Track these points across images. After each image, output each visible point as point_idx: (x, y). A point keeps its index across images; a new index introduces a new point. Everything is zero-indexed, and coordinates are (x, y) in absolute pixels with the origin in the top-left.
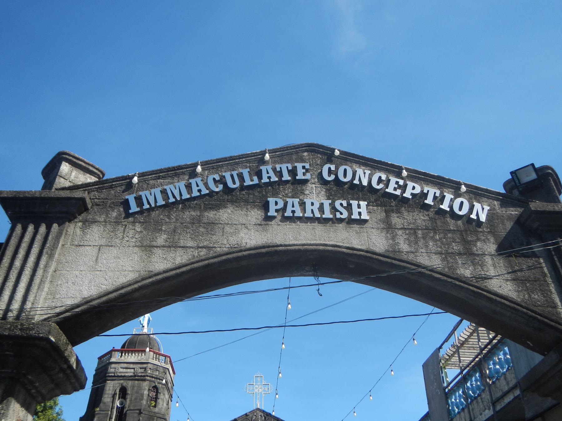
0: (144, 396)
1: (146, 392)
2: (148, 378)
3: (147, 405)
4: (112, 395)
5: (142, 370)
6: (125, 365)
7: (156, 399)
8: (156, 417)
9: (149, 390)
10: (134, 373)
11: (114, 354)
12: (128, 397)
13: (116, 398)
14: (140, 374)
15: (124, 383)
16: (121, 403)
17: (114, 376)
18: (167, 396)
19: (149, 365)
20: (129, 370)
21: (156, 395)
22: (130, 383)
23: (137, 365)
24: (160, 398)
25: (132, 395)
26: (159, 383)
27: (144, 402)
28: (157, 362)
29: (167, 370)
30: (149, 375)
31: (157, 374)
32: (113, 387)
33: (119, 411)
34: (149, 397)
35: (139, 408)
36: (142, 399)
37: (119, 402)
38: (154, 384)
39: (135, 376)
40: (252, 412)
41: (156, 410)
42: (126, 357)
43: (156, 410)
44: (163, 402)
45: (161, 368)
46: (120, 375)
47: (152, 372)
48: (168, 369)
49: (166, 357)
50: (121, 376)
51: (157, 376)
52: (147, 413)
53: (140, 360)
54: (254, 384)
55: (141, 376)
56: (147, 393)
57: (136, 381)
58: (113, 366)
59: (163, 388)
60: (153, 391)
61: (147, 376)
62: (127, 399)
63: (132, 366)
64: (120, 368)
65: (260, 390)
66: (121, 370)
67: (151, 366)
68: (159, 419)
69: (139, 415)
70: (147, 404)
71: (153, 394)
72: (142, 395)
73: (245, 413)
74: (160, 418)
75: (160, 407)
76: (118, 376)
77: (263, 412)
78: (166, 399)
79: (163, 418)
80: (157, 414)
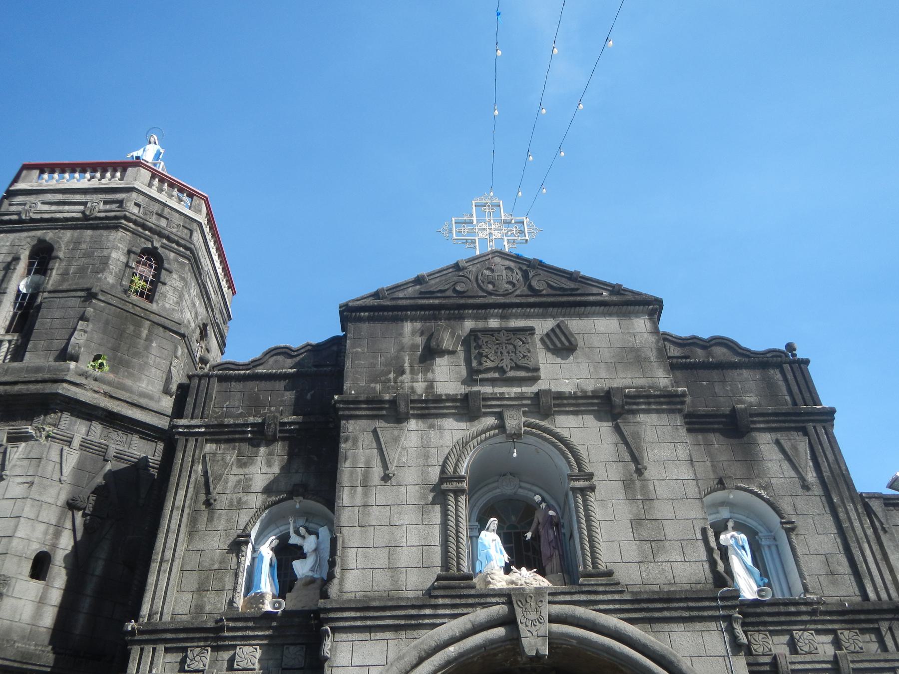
0: (110, 262)
1: (118, 256)
2: (131, 225)
3: (119, 287)
4: (4, 265)
5: (114, 206)
6: (59, 197)
7: (156, 282)
8: (149, 322)
9: (129, 252)
10: (83, 213)
11: (26, 176)
13: (15, 269)
14: (102, 215)
15: (49, 235)
16: (36, 290)
17: (20, 221)
18: (201, 310)
19: (134, 195)
20: (67, 208)
21: (157, 276)
22: (68, 234)
23: (95, 196)
24: (169, 283)
25: (70, 260)
26: (166, 248)
27: (111, 280)
28: (162, 197)
29: (195, 226)
30: (134, 217)
31: (163, 223)
32: (12, 246)
33: (21, 305)
34: (128, 270)
35: (86, 286)
36: (102, 271)
37: (27, 282)
38: (150, 243)
39: (86, 217)
40: (476, 261)
41: (154, 307)
42: (65, 180)
43: (154, 307)
44: (181, 297)
45: (177, 215)
46: (38, 216)
47: (145, 214)
48: (200, 225)
49: (195, 197)
50: (42, 220)
51: (162, 230)
52: (114, 302)
54: (475, 219)
55: (107, 218)
56: (123, 259)
57: (89, 231)
58: (20, 199)
59: (182, 265)
60: (144, 264)
61: (126, 218)
62: (52, 269)
63: (78, 198)
64: (39, 204)
65: (497, 235)
66: (40, 207)
68: (161, 328)
69: (83, 301)
70: (121, 285)
71: (148, 272)
72: (105, 262)
73: (452, 262)
74: (165, 328)
75: (167, 306)
76: (32, 220)
77: (518, 259)
78: (194, 305)
79: (174, 329)
80: (152, 315)
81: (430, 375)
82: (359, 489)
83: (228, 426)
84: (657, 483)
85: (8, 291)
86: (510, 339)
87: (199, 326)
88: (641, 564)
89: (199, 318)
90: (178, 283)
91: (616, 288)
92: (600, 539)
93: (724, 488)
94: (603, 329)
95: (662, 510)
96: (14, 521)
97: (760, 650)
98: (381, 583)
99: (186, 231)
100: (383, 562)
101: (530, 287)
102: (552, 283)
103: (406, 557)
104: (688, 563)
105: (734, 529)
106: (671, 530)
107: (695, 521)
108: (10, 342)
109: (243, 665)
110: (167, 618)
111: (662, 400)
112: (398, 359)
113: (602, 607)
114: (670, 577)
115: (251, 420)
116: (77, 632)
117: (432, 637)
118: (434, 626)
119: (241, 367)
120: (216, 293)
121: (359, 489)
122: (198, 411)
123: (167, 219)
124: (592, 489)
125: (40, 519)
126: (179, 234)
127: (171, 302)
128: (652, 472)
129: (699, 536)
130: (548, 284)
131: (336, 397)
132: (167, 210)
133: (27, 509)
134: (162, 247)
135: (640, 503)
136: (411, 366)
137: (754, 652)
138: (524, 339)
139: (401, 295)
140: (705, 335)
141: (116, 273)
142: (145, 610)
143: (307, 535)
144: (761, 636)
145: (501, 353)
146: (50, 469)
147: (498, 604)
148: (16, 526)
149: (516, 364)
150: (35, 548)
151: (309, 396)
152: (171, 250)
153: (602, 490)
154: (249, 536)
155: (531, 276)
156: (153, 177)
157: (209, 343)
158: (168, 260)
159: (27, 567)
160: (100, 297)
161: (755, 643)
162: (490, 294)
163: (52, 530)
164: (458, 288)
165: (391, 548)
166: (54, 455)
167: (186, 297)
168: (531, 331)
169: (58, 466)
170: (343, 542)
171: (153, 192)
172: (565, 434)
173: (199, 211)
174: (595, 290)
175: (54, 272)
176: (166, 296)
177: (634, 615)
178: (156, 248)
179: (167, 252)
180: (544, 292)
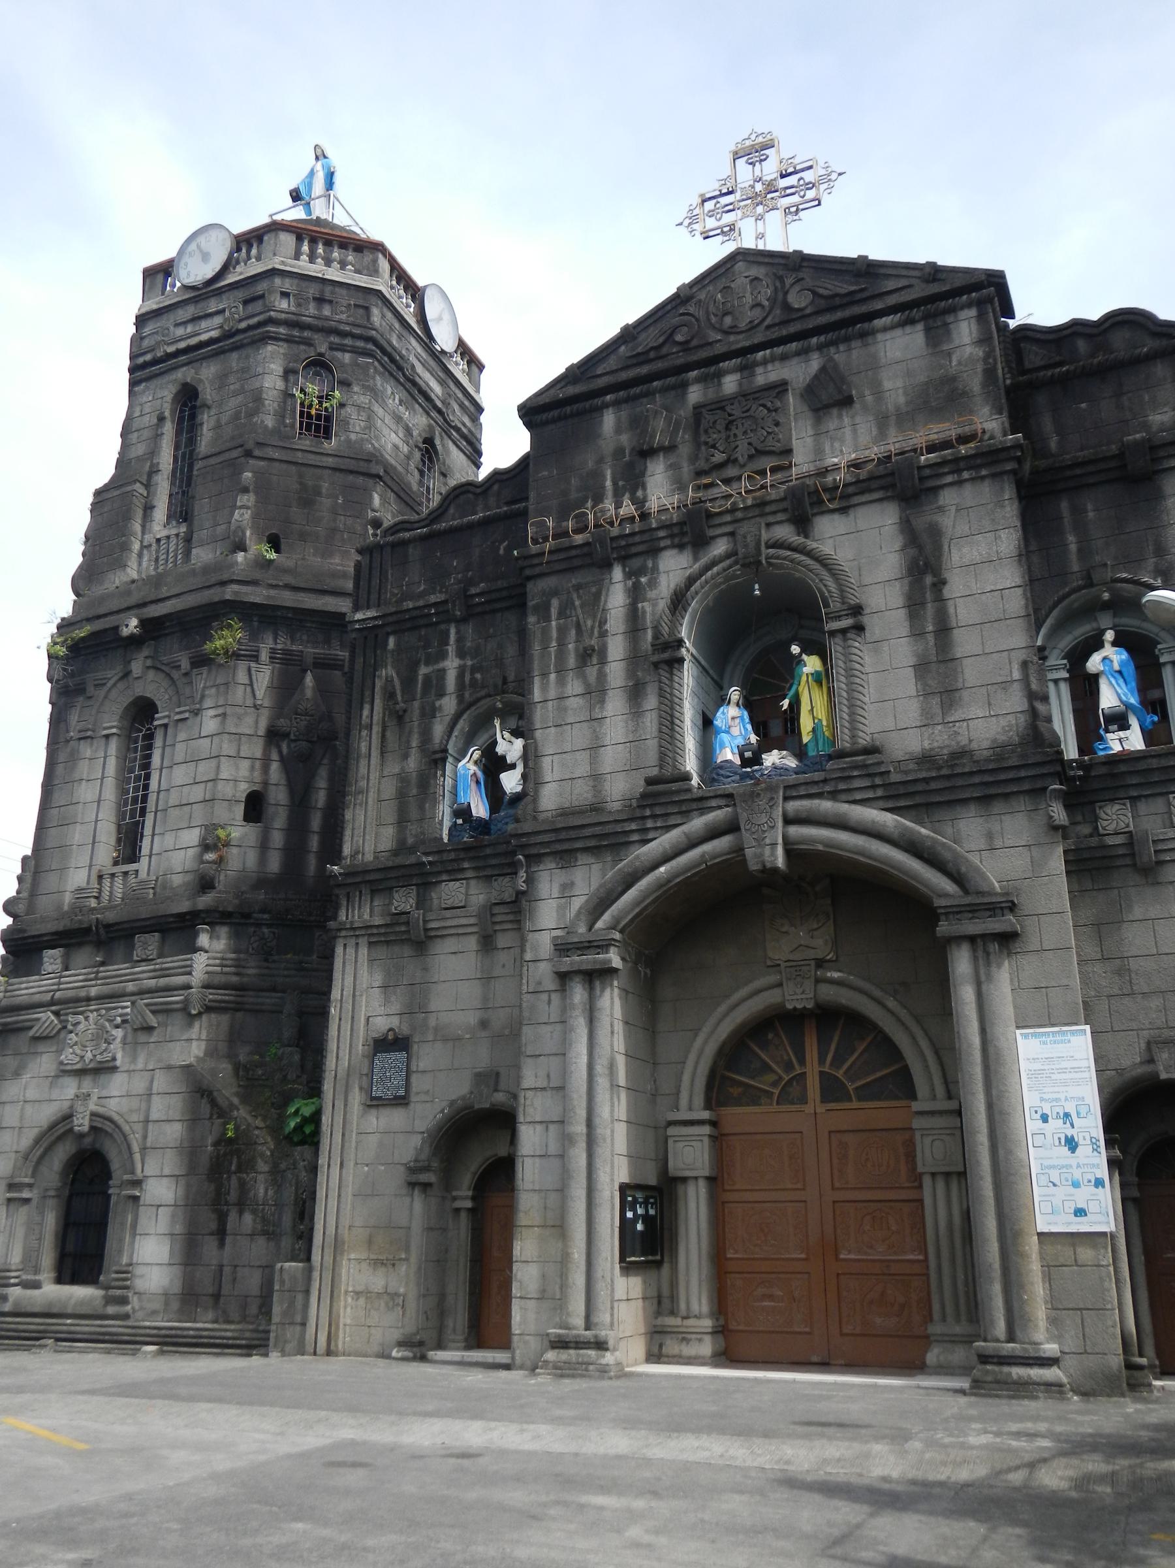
0: (264, 396)
5: (257, 306)
12: (207, 422)
14: (243, 325)
19: (278, 281)
26: (337, 350)
27: (270, 422)
28: (317, 269)
30: (283, 316)
34: (289, 402)
45: (344, 292)
47: (299, 305)
48: (378, 293)
53: (241, 274)
55: (250, 328)
56: (280, 384)
61: (271, 321)
62: (202, 424)
67: (287, 285)
75: (353, 437)
78: (398, 419)
81: (640, 493)
82: (553, 676)
83: (408, 610)
84: (960, 602)
85: (161, 467)
86: (748, 411)
87: (417, 446)
88: (924, 729)
89: (415, 433)
90: (362, 398)
91: (927, 270)
92: (866, 700)
93: (1092, 585)
94: (898, 355)
95: (965, 643)
96: (214, 762)
97: (1111, 828)
98: (581, 794)
99: (361, 311)
100: (583, 769)
101: (787, 307)
102: (821, 291)
103: (612, 757)
104: (994, 719)
105: (1115, 644)
106: (971, 673)
107: (1013, 653)
108: (177, 535)
109: (449, 903)
110: (369, 857)
111: (979, 461)
112: (597, 475)
113: (858, 796)
114: (964, 741)
115: (433, 599)
116: (312, 874)
117: (637, 857)
118: (646, 842)
119: (417, 525)
120: (442, 383)
121: (553, 676)
122: (374, 597)
123: (331, 302)
124: (860, 628)
125: (242, 755)
126: (351, 319)
127: (358, 429)
128: (957, 586)
129: (1016, 675)
130: (814, 293)
131: (515, 552)
132: (328, 289)
133: (225, 746)
134: (331, 349)
135: (931, 639)
136: (615, 484)
137: (1101, 831)
138: (769, 405)
139: (599, 372)
140: (1094, 314)
141: (275, 411)
142: (347, 850)
143: (513, 739)
144: (1117, 807)
145: (735, 435)
146: (239, 694)
147: (720, 807)
148: (218, 767)
149: (756, 449)
150: (244, 789)
151: (501, 552)
152: (342, 348)
153: (874, 626)
154: (445, 751)
155: (787, 286)
156: (300, 239)
157: (444, 463)
158: (343, 365)
159: (240, 810)
160: (257, 453)
161: (1105, 817)
162: (726, 333)
163: (258, 764)
164: (679, 338)
165: (595, 748)
166: (242, 677)
167: (380, 411)
168: (780, 388)
169: (249, 689)
170: (536, 750)
171: (303, 266)
172: (826, 549)
173: (374, 272)
174: (891, 285)
175: (205, 427)
176: (348, 423)
177: (902, 803)
178: (321, 355)
179: (339, 354)
180: (808, 311)
